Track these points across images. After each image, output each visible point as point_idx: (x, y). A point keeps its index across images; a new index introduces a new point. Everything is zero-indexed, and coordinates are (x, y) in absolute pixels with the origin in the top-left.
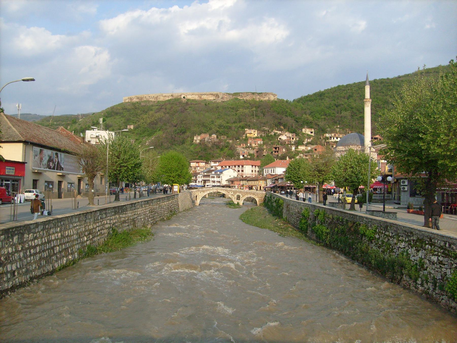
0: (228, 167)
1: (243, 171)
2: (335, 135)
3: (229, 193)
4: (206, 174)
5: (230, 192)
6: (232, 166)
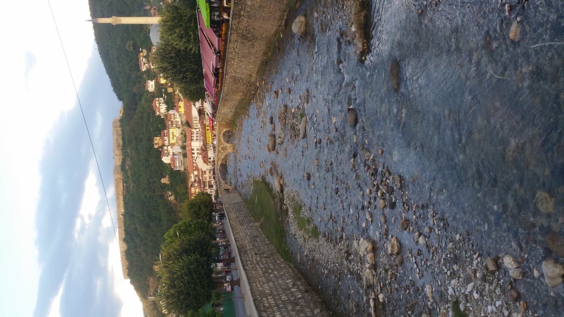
3: (220, 158)
4: (202, 186)
5: (219, 157)
6: (193, 160)
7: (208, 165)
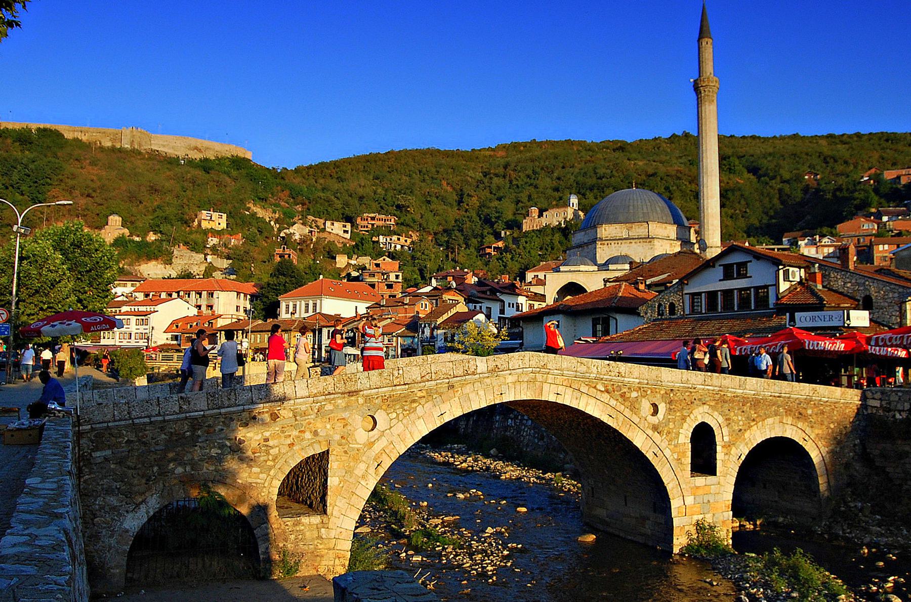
0: (175, 295)
1: (210, 307)
2: (399, 239)
3: (634, 407)
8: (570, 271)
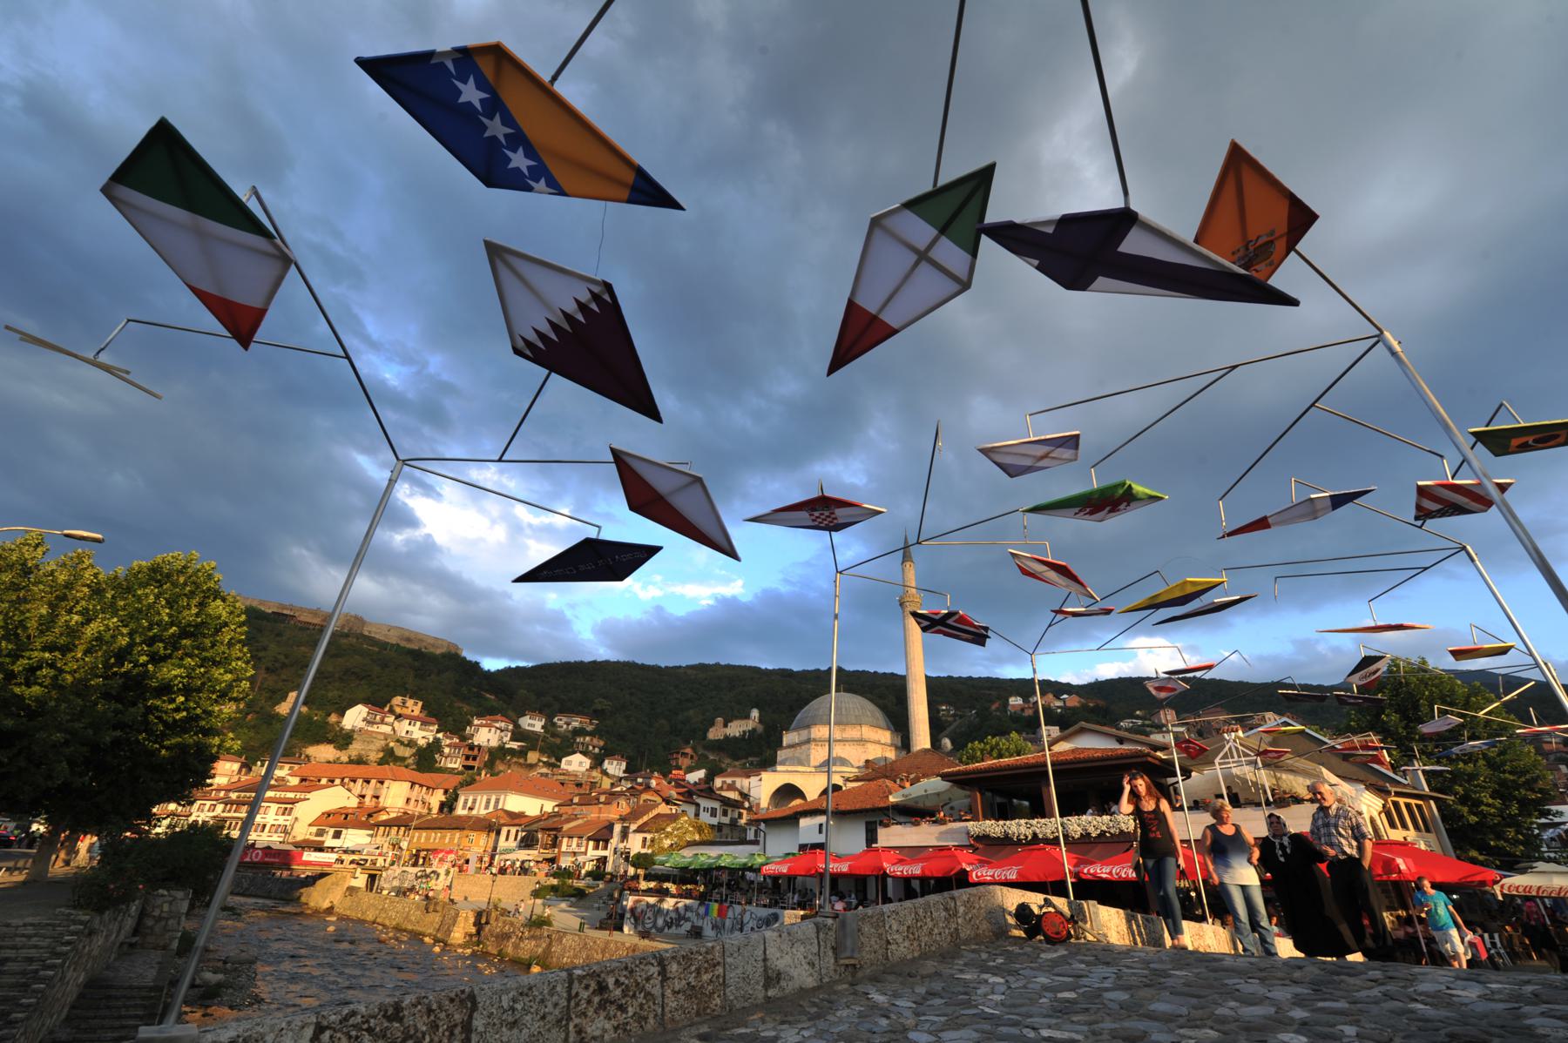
0: (338, 781)
4: (234, 796)
7: (310, 825)
8: (788, 771)
